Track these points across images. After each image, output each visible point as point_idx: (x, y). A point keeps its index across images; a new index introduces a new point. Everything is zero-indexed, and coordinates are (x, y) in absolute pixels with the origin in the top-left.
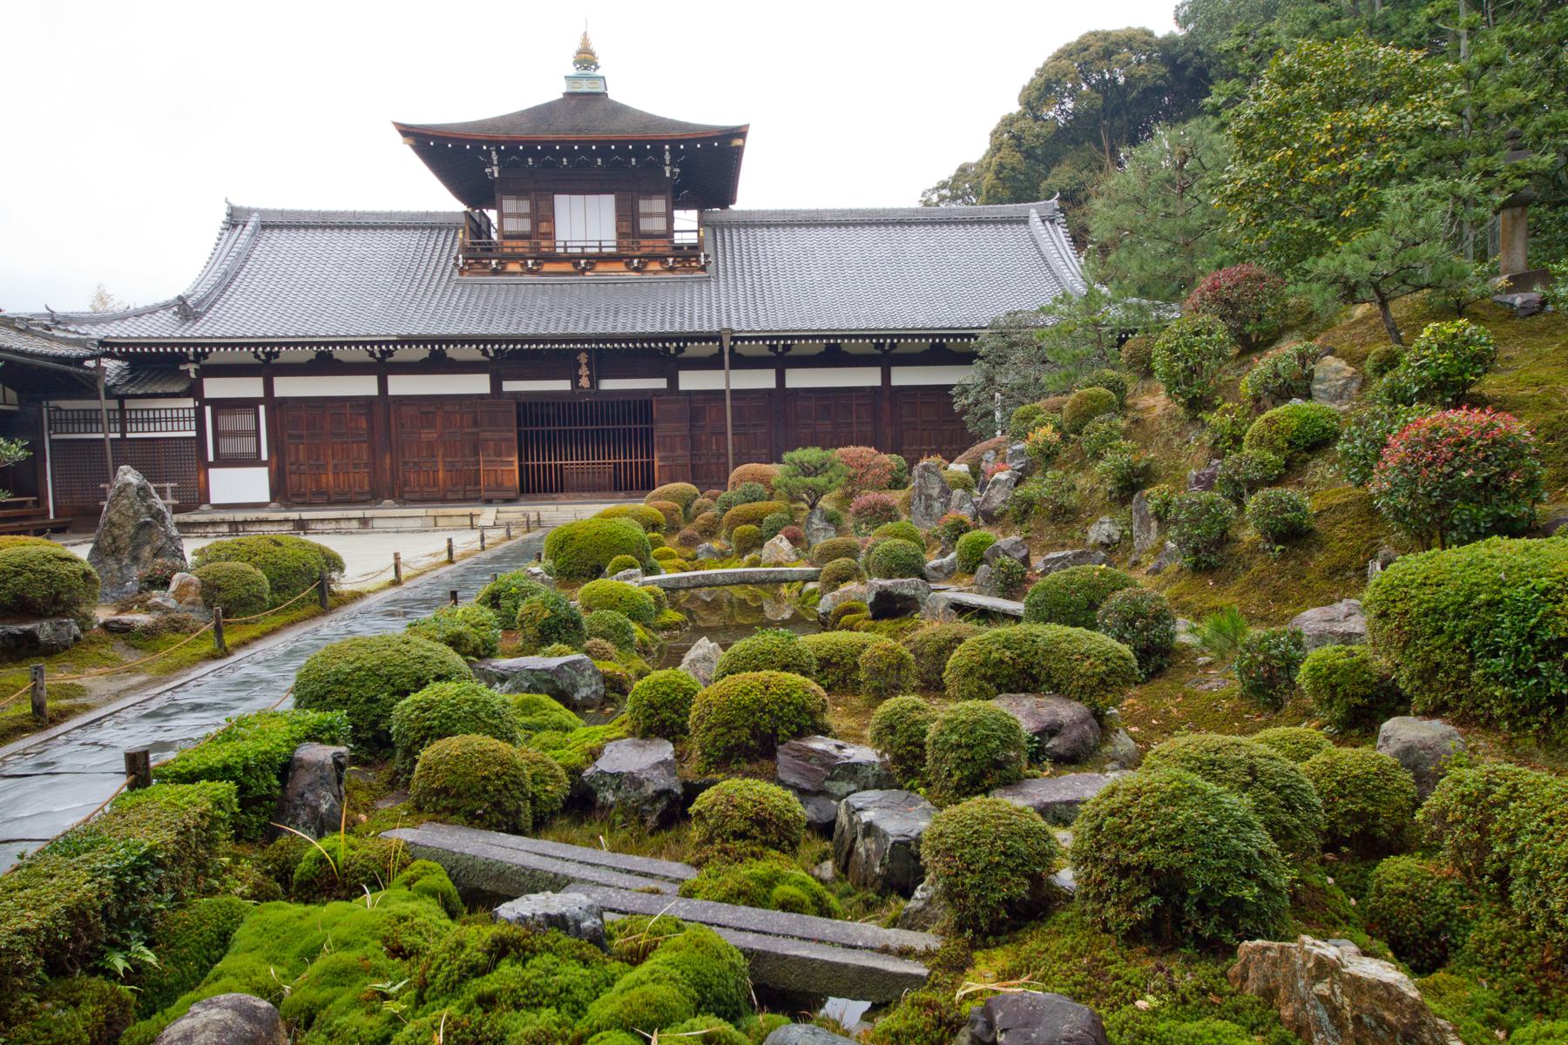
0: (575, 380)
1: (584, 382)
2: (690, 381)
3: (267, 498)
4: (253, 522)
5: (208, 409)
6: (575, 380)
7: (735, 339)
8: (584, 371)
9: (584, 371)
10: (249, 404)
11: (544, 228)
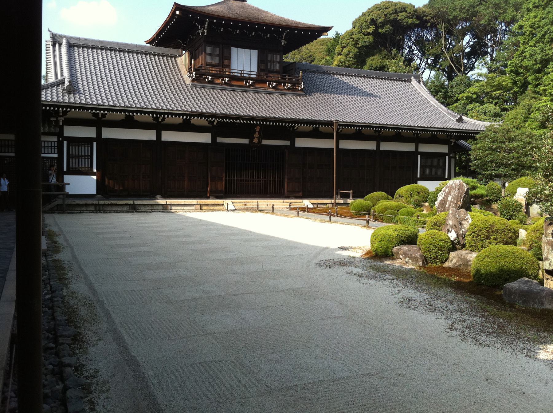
0: (251, 138)
1: (256, 141)
2: (301, 143)
3: (95, 193)
4: (108, 205)
5: (65, 143)
6: (251, 138)
7: (340, 125)
8: (257, 135)
9: (257, 135)
10: (88, 141)
11: (226, 62)
